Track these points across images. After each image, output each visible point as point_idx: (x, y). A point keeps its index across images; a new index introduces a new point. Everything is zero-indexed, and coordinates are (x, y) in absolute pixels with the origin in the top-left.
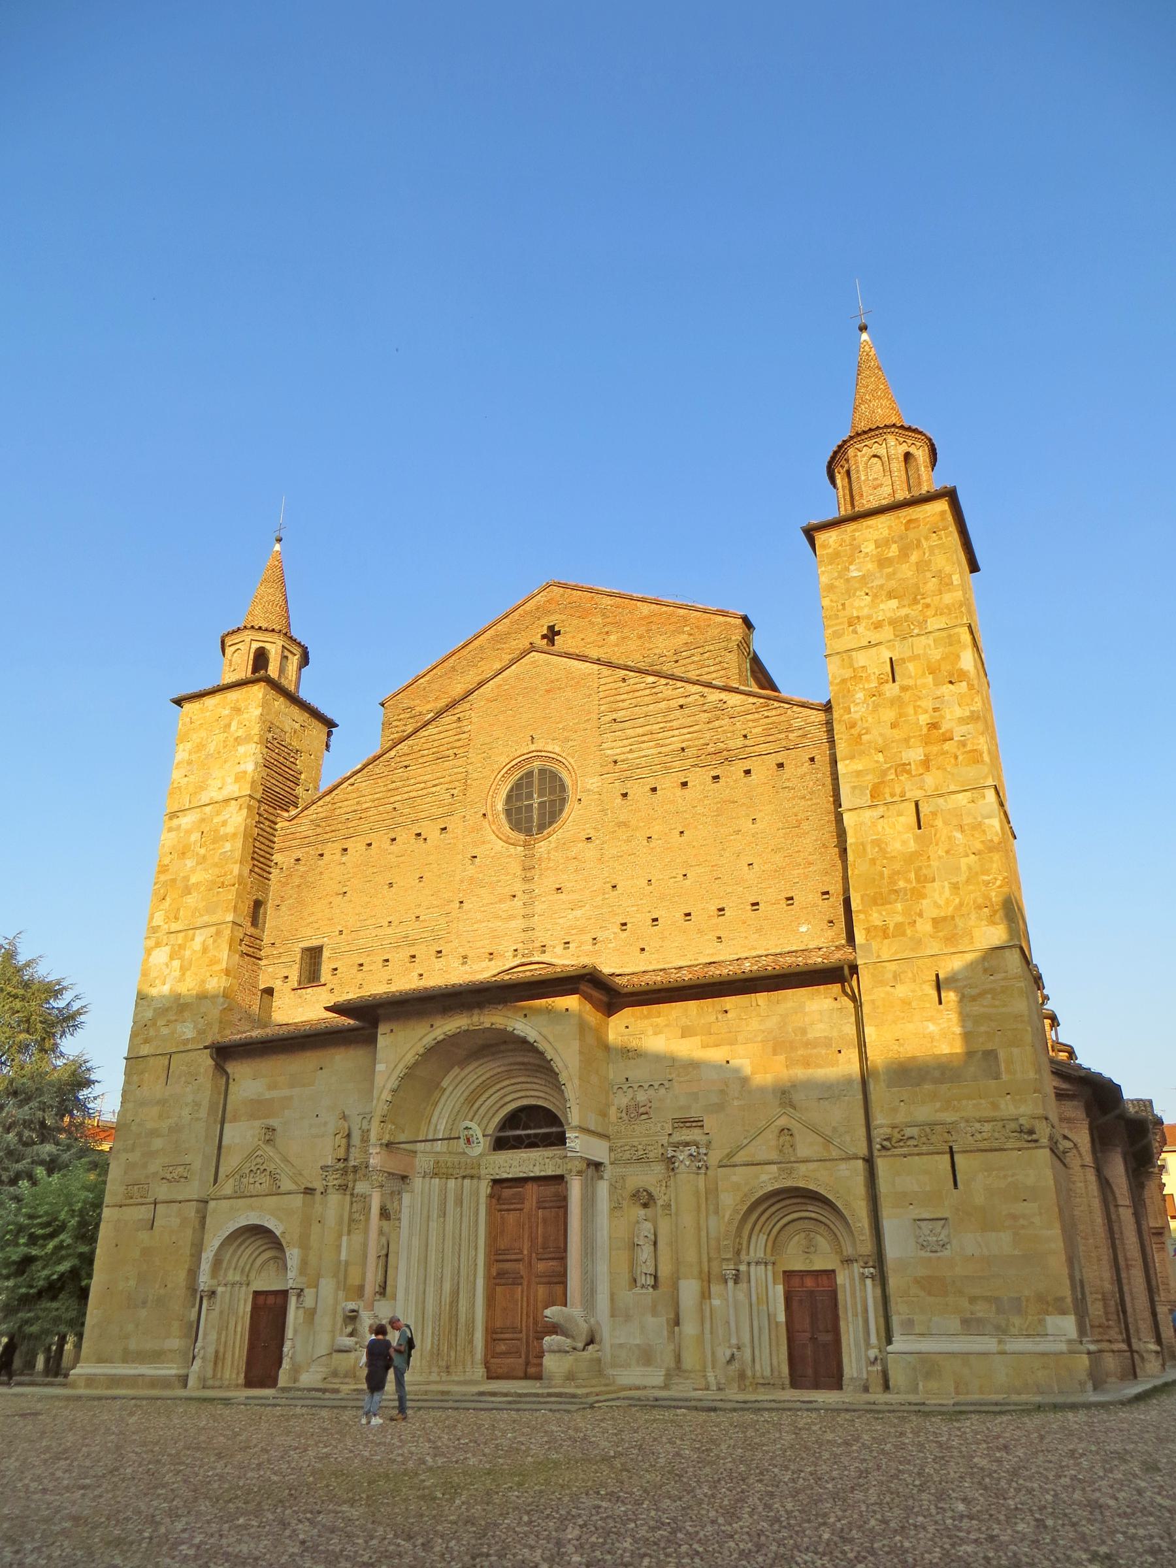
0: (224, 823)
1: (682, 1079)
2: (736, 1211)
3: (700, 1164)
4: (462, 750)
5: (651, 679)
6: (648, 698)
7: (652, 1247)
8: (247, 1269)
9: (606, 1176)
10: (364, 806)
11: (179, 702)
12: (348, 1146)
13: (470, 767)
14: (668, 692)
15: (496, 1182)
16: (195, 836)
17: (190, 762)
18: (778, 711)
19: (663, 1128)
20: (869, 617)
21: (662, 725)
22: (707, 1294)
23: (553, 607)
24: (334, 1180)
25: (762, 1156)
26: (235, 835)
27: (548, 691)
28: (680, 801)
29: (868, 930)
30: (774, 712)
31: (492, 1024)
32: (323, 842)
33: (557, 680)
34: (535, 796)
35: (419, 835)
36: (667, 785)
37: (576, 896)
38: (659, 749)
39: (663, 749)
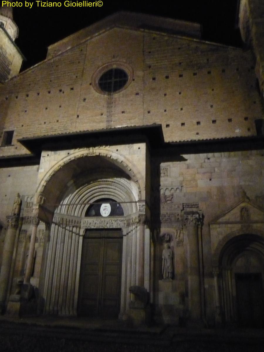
12: (20, 209)
19: (178, 207)
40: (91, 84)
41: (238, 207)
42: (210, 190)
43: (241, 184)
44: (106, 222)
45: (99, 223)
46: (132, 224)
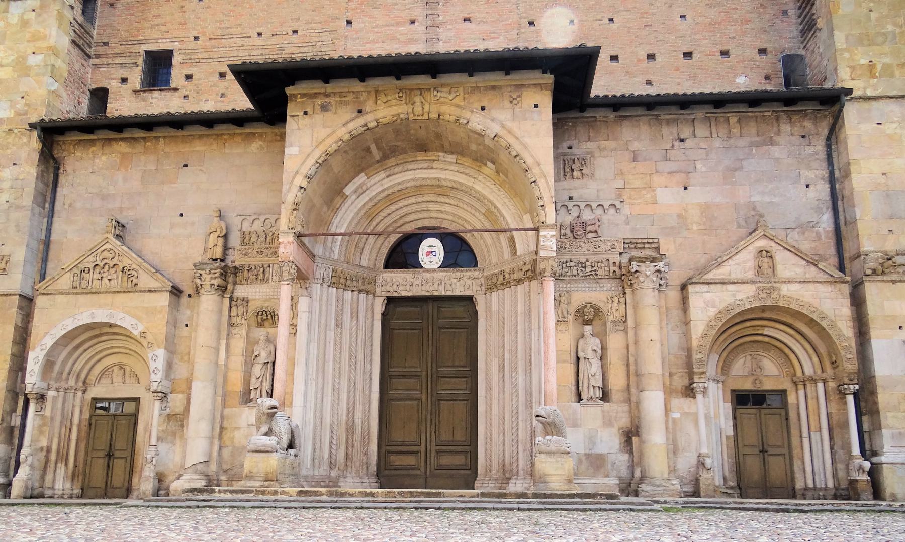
1: (634, 201)
8: (83, 376)
12: (226, 248)
15: (392, 301)
19: (613, 247)
24: (210, 279)
25: (737, 275)
41: (750, 247)
43: (753, 199)
45: (420, 284)
46: (503, 284)
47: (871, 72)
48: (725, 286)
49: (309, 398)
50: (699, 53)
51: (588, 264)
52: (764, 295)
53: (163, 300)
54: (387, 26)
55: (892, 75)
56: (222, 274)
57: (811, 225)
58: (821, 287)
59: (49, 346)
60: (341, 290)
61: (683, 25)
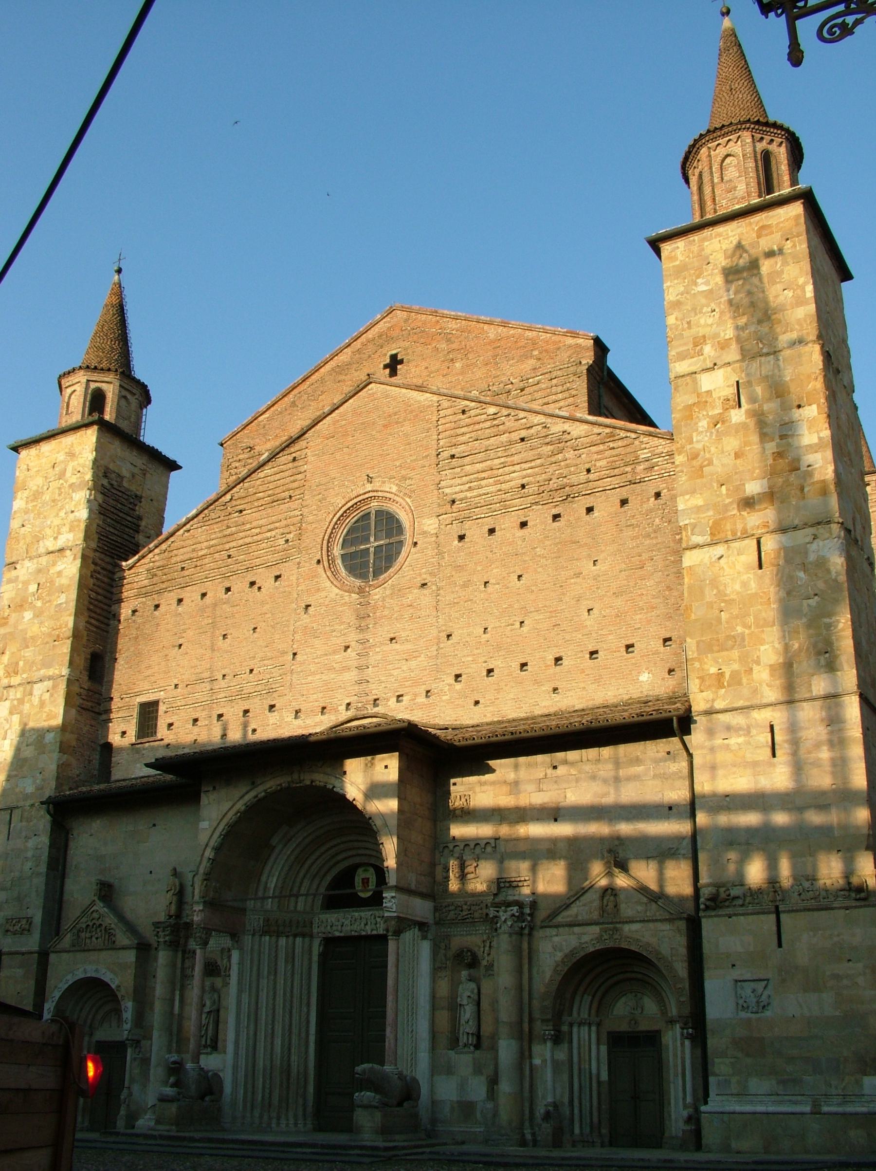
0: (60, 573)
2: (555, 971)
3: (524, 924)
4: (298, 492)
5: (492, 410)
6: (488, 431)
7: (475, 1008)
9: (430, 936)
10: (200, 553)
11: (16, 449)
13: (305, 510)
14: (510, 424)
15: (330, 942)
16: (33, 588)
17: (26, 512)
18: (625, 442)
20: (716, 335)
21: (502, 460)
22: (527, 1053)
23: (395, 333)
25: (584, 916)
26: (69, 586)
27: (385, 426)
28: (519, 543)
29: (702, 679)
30: (620, 443)
31: (312, 782)
32: (159, 592)
33: (395, 414)
34: (372, 539)
35: (252, 584)
36: (507, 525)
37: (409, 646)
38: (499, 487)
39: (504, 486)
40: (319, 562)
42: (555, 845)
44: (364, 921)
47: (719, 681)
48: (571, 929)
49: (240, 1046)
50: (605, 650)
51: (465, 907)
52: (606, 937)
53: (130, 957)
54: (326, 655)
55: (740, 683)
56: (172, 931)
57: (672, 851)
58: (659, 926)
59: (57, 998)
60: (274, 939)
61: (590, 621)
